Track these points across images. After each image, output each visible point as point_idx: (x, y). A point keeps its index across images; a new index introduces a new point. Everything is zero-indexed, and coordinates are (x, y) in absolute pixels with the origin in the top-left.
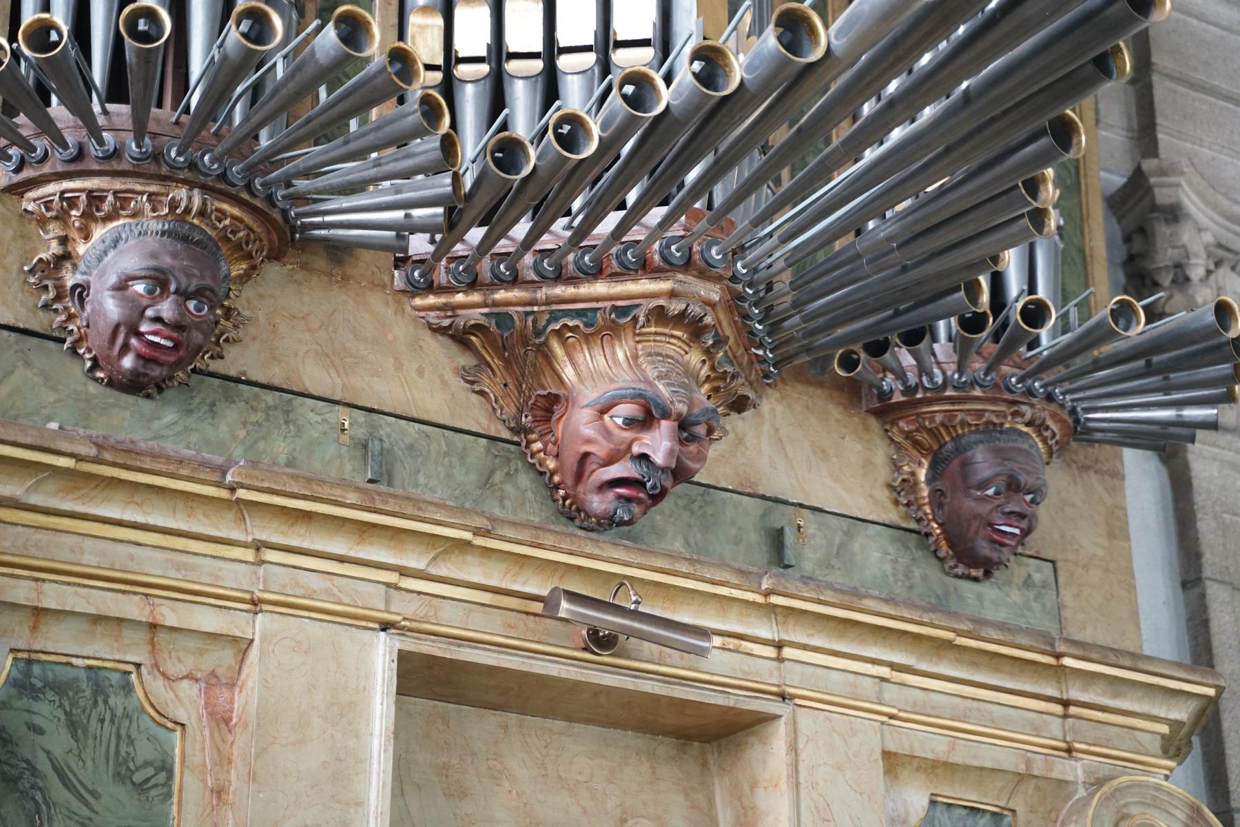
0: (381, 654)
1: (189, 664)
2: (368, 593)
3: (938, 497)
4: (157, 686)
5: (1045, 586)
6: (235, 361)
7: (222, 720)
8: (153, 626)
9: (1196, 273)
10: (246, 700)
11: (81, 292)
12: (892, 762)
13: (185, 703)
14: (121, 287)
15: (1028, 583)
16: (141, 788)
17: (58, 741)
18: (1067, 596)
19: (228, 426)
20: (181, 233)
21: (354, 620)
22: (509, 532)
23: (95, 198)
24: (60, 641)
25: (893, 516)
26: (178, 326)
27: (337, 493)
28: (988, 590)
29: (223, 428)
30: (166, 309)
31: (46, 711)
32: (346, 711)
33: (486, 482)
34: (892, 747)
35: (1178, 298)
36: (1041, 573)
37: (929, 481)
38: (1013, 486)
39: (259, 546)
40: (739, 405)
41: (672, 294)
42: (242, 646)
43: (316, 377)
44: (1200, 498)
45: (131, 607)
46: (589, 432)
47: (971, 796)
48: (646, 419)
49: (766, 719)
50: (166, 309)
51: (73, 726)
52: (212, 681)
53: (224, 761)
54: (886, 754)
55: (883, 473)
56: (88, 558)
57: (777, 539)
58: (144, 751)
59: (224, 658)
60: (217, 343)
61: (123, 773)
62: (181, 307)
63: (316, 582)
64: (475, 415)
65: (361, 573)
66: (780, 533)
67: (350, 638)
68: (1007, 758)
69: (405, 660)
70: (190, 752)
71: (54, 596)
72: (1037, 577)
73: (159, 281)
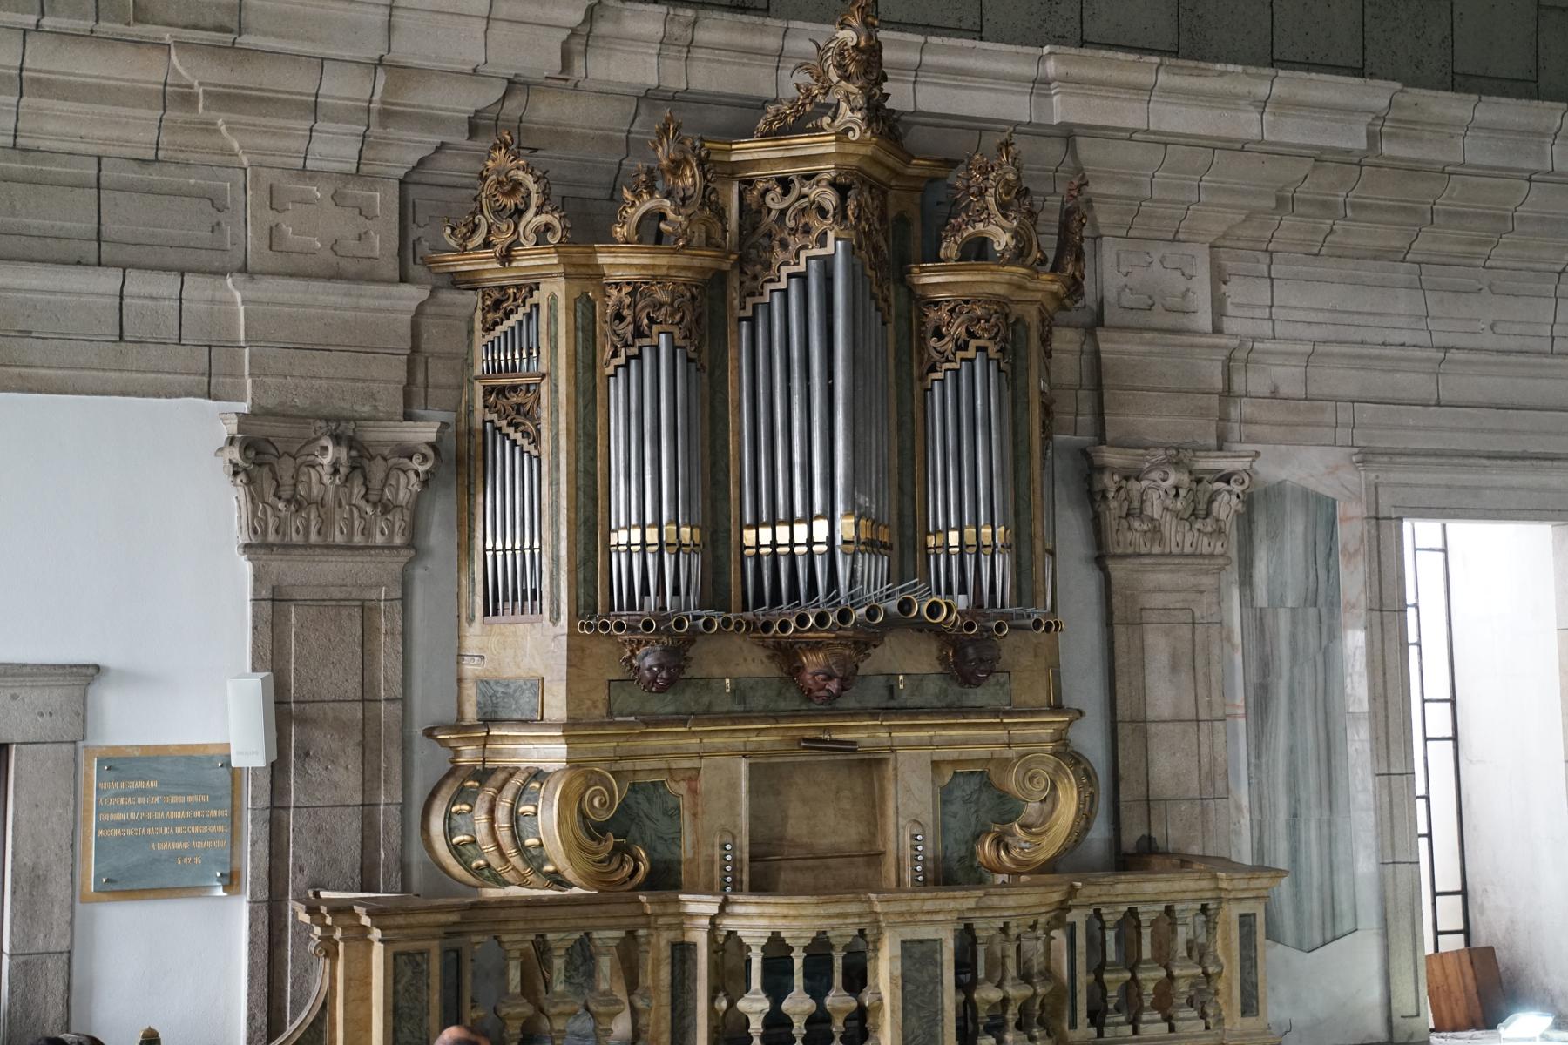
0: (743, 765)
2: (738, 741)
4: (673, 785)
6: (691, 672)
7: (694, 792)
9: (1111, 495)
10: (702, 785)
11: (638, 669)
12: (936, 765)
13: (681, 788)
14: (650, 668)
15: (997, 683)
17: (645, 806)
18: (1014, 686)
19: (688, 695)
20: (665, 650)
23: (639, 642)
24: (642, 778)
25: (940, 669)
28: (979, 691)
30: (664, 674)
31: (640, 797)
32: (733, 786)
33: (779, 694)
35: (1103, 506)
36: (1003, 678)
38: (982, 660)
42: (699, 770)
43: (717, 671)
44: (1113, 588)
45: (662, 764)
48: (830, 677)
49: (880, 762)
51: (649, 800)
52: (690, 779)
53: (696, 805)
55: (935, 652)
58: (671, 804)
60: (681, 669)
61: (665, 812)
62: (668, 672)
64: (774, 671)
65: (738, 741)
67: (732, 761)
69: (751, 767)
70: (685, 803)
71: (639, 765)
73: (661, 667)
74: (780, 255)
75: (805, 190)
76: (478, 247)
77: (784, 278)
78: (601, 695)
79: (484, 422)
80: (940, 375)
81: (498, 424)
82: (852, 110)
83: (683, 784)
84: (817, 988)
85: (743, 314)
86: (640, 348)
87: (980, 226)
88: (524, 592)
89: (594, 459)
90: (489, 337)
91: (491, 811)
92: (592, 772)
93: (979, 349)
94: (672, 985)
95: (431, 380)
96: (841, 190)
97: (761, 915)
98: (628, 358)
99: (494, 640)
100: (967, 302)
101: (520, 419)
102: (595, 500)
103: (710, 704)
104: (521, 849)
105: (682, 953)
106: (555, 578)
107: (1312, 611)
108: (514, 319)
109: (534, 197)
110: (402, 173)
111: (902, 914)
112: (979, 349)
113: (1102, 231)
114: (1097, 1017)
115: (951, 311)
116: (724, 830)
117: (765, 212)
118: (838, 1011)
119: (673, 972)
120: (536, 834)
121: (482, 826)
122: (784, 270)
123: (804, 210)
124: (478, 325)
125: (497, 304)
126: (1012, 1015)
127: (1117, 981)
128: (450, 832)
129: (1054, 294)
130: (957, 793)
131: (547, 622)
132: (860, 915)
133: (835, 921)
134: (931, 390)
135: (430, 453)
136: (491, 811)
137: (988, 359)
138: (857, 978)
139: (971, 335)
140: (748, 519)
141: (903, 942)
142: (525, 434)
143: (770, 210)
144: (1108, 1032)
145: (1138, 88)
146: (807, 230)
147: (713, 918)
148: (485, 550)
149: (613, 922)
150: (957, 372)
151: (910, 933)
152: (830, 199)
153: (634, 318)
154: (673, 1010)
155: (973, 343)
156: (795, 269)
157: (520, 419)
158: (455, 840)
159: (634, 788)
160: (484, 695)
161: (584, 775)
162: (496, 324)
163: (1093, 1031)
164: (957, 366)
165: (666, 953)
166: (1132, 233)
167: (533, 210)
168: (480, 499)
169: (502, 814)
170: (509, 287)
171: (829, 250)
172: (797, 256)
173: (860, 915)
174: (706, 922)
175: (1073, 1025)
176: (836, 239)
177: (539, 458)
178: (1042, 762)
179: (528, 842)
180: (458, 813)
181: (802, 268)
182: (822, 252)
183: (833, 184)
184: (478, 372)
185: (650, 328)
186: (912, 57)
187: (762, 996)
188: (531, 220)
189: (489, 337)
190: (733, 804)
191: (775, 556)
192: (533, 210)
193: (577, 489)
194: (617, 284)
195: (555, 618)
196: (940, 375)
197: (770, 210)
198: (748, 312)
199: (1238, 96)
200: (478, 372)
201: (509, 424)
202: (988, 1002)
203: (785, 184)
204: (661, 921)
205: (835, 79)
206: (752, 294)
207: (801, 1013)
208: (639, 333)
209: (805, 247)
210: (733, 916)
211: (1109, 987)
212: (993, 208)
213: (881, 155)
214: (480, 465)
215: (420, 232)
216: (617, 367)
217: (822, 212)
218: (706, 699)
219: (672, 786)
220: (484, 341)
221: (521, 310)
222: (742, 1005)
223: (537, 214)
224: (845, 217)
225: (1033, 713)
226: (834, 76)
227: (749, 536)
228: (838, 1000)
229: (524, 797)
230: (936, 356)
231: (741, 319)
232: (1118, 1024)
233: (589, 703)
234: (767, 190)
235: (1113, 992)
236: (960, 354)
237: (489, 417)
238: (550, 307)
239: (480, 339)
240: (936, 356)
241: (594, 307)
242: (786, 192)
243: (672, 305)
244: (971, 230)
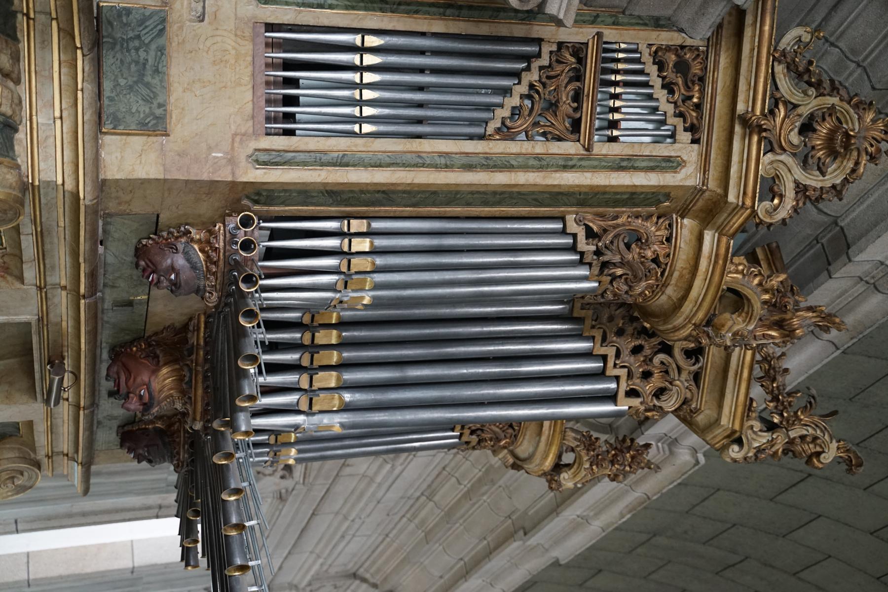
46: (139, 380)
69: (28, 324)
75: (684, 376)
79: (539, 41)
81: (536, 64)
87: (587, 465)
98: (582, 254)
100: (516, 436)
107: (164, 485)
123: (667, 372)
124: (666, 38)
125: (682, 67)
148: (365, 32)
160: (142, 22)
162: (661, 66)
168: (438, 26)
170: (702, 92)
177: (482, 137)
182: (622, 394)
184: (610, 34)
188: (792, 174)
199: (597, 515)
200: (610, 34)
201: (531, 86)
214: (484, 29)
216: (575, 236)
220: (643, 47)
223: (797, 184)
237: (546, 49)
239: (647, 39)
244: (586, 458)
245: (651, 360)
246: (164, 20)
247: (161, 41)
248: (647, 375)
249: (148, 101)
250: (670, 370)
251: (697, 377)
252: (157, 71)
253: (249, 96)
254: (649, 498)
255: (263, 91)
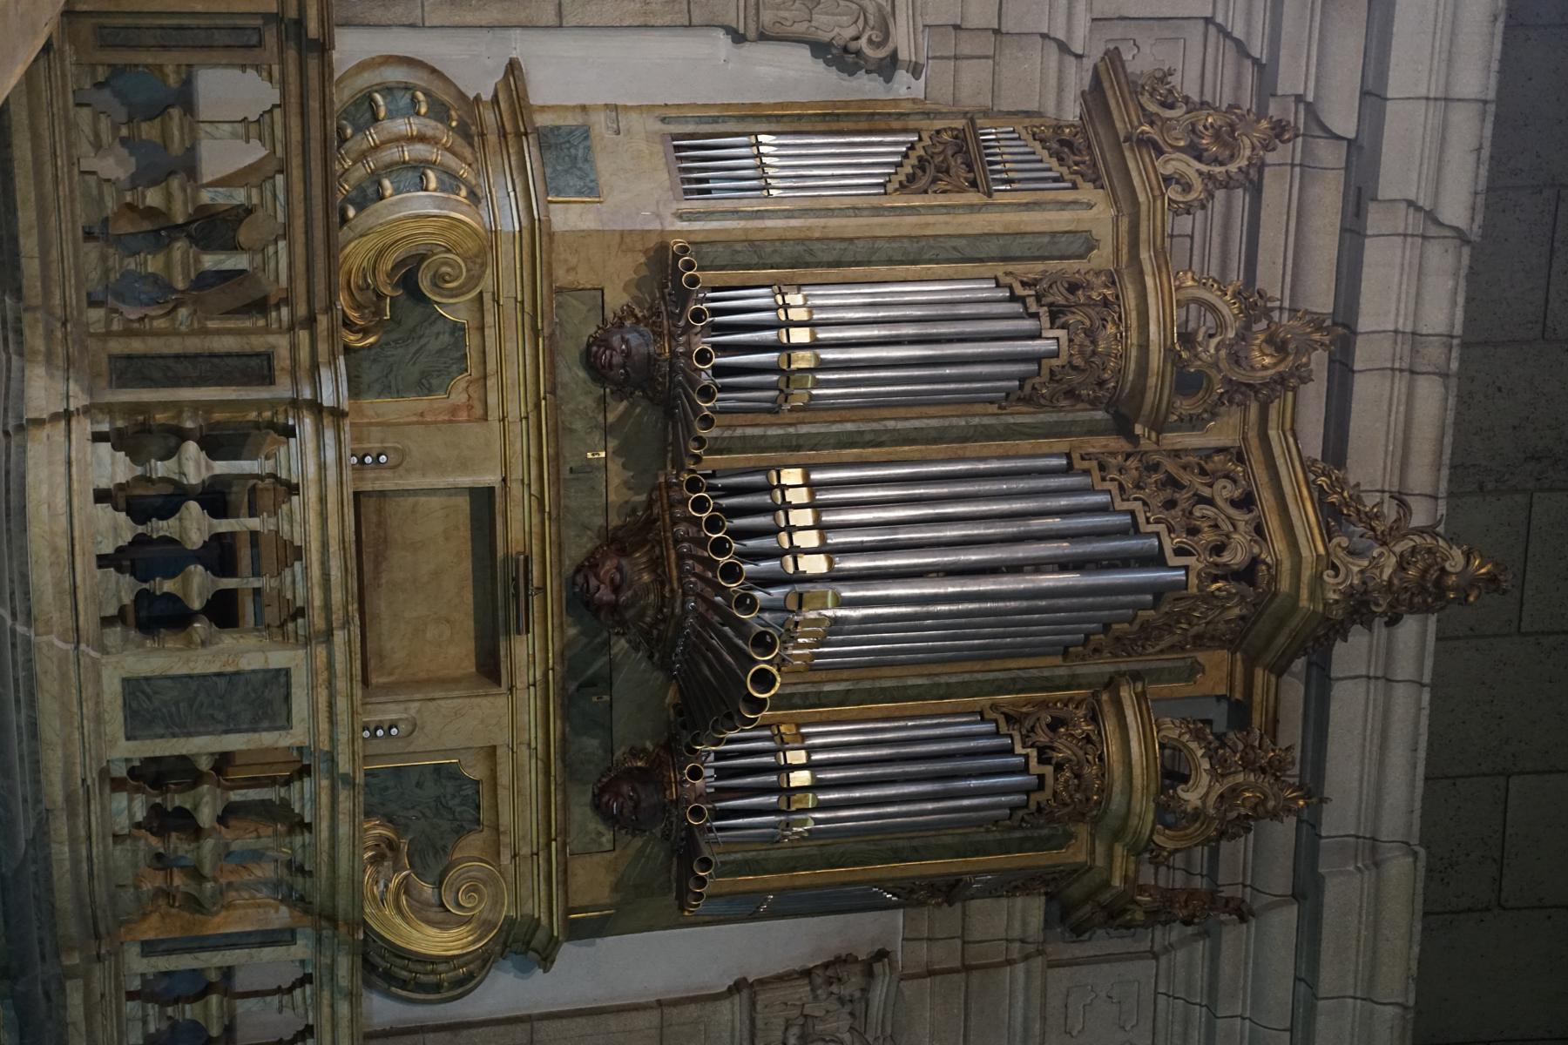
0: (491, 478)
1: (475, 396)
3: (630, 771)
4: (463, 384)
5: (601, 844)
8: (485, 377)
12: (492, 752)
13: (458, 397)
14: (624, 340)
15: (600, 834)
16: (420, 383)
21: (505, 464)
22: (554, 529)
24: (472, 341)
26: (611, 366)
27: (552, 444)
28: (589, 812)
29: (582, 398)
31: (446, 338)
32: (464, 466)
34: (499, 752)
36: (607, 839)
37: (638, 768)
39: (527, 418)
40: (651, 657)
41: (672, 591)
44: (709, 1007)
45: (492, 366)
47: (485, 803)
48: (616, 589)
50: (617, 359)
51: (440, 351)
54: (494, 748)
56: (508, 345)
57: (591, 683)
58: (434, 382)
59: (478, 411)
61: (425, 375)
63: (518, 445)
66: (595, 685)
68: (505, 818)
69: (491, 489)
71: (490, 333)
72: (604, 840)
74: (1156, 502)
76: (1143, 109)
77: (1126, 506)
78: (584, 279)
79: (918, 131)
80: (1004, 729)
81: (919, 146)
82: (1362, 572)
83: (464, 397)
84: (220, 555)
85: (1076, 456)
86: (1035, 316)
88: (706, 180)
89: (891, 262)
90: (1024, 134)
91: (421, 138)
92: (484, 265)
93: (1041, 777)
94: (212, 355)
95: (965, 63)
96: (1248, 573)
97: (322, 467)
98: (1022, 300)
99: (643, 146)
100: (1101, 758)
101: (931, 171)
102: (838, 264)
103: (572, 431)
104: (375, 178)
105: (259, 369)
106: (736, 214)
108: (1054, 163)
109: (1222, 169)
110: (1219, 19)
111: (330, 665)
112: (1041, 777)
113: (1163, 959)
114: (153, 992)
115: (1088, 739)
116: (403, 454)
117: (1207, 480)
118: (186, 585)
119: (229, 355)
120: (397, 191)
121: (401, 126)
122: (1137, 506)
123: (1216, 526)
126: (178, 845)
127: (207, 1017)
128: (387, 90)
129: (1107, 884)
130: (450, 787)
131: (675, 206)
132: (327, 606)
133: (316, 571)
134: (983, 720)
135: (882, 53)
136: (421, 138)
137: (1028, 793)
138: (223, 611)
139: (1059, 767)
140: (816, 476)
141: (287, 672)
142: (911, 178)
143: (1211, 486)
144: (132, 1008)
145: (1371, 981)
146: (1193, 531)
147: (316, 407)
149: (300, 266)
150: (1009, 751)
151: (299, 680)
152: (1235, 557)
153: (1077, 305)
154: (177, 357)
155: (1048, 770)
156: (1141, 519)
157: (931, 171)
158: (378, 97)
159: (457, 329)
160: (571, 133)
161: (482, 252)
163: (136, 984)
164: (1019, 749)
165: (258, 343)
166: (1162, 1000)
167: (1204, 168)
169: (421, 150)
171: (1173, 561)
172: (1158, 521)
173: (327, 606)
174: (307, 394)
175: (149, 949)
176: (1186, 568)
178: (497, 902)
179: (387, 183)
180: (414, 98)
181: (1144, 528)
182: (1168, 552)
183: (1255, 561)
185: (1063, 327)
186: (1405, 668)
187: (205, 475)
189: (1024, 134)
190: (439, 466)
191: (771, 510)
192: (1204, 168)
193: (851, 240)
194: (1114, 283)
195: (680, 216)
196: (1004, 729)
197: (1211, 486)
198: (1079, 464)
201: (920, 159)
202: (196, 807)
203: (1246, 502)
204: (303, 335)
205: (1398, 549)
206: (1102, 467)
207: (183, 529)
208: (1055, 314)
209: (1170, 530)
210: (319, 433)
211: (198, 1006)
212: (1230, 782)
213: (1295, 622)
215: (1146, 49)
216: (1011, 288)
217: (1218, 549)
218: (578, 425)
219: (461, 382)
220: (1019, 128)
221: (1065, 170)
222: (191, 447)
223: (1200, 173)
224: (1215, 579)
225: (565, 883)
226: (1403, 546)
227: (792, 476)
228: (197, 585)
229: (445, 177)
230: (1028, 724)
231: (1068, 456)
232: (145, 1022)
233: (573, 260)
234: (1235, 481)
235: (190, 1011)
236: (1033, 753)
237: (925, 136)
238: (1075, 202)
240: (1028, 724)
241: (1080, 257)
242: (1234, 503)
243: (1094, 353)
244: (1200, 753)
245: (1191, 513)
246: (587, 131)
247: (587, 143)
248: (1193, 531)
249: (580, 178)
250: (1221, 524)
251: (1259, 530)
252: (586, 160)
253: (666, 176)
254: (1405, 1008)
255: (676, 173)
